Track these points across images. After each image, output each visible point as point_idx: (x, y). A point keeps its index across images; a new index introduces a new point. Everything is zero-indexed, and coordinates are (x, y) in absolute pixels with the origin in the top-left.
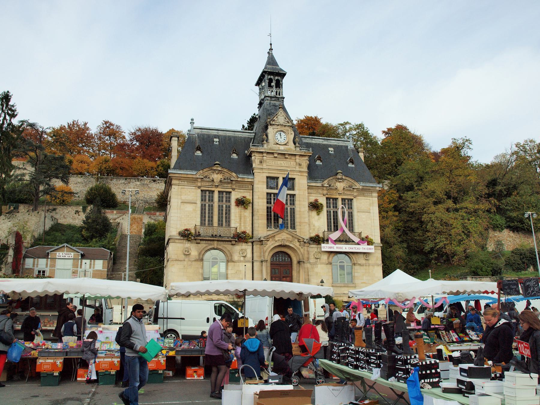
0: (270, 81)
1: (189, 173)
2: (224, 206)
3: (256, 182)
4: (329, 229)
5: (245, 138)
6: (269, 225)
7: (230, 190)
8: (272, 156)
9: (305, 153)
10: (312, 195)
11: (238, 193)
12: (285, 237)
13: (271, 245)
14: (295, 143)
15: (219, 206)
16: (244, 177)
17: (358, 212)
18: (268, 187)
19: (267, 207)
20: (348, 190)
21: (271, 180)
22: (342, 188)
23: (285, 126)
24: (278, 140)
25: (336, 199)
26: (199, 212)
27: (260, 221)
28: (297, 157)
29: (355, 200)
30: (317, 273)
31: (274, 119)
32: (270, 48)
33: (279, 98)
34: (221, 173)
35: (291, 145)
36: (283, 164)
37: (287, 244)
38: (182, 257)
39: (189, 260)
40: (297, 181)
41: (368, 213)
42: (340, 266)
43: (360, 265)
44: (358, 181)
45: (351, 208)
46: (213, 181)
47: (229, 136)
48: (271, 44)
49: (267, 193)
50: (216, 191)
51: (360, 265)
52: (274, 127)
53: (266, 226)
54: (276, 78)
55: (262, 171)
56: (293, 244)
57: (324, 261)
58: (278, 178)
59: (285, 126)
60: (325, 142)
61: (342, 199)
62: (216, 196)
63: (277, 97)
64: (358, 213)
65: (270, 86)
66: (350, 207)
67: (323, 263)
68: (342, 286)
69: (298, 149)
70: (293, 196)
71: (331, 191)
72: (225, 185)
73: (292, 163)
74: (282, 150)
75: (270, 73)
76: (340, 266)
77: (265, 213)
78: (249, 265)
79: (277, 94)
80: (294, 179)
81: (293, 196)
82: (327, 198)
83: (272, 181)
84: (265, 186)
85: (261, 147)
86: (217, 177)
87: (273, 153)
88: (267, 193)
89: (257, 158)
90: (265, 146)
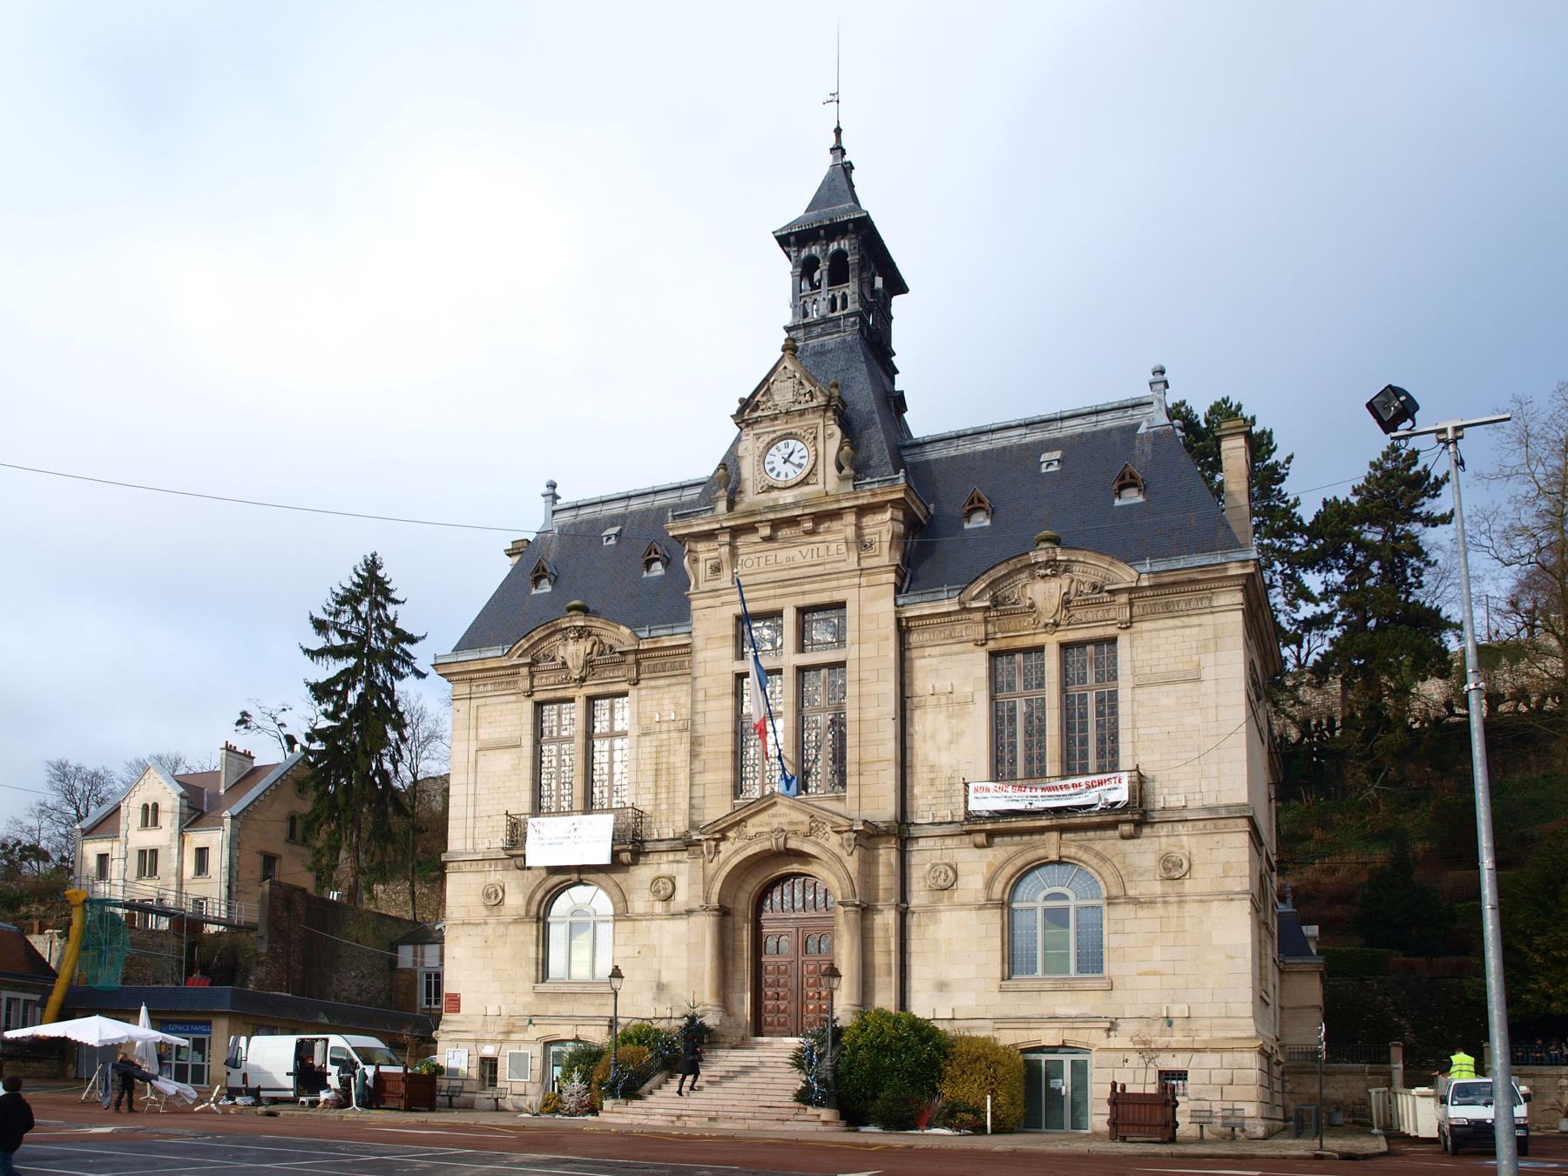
1: (489, 654)
3: (698, 641)
8: (755, 538)
9: (874, 495)
10: (928, 651)
11: (649, 692)
12: (783, 820)
14: (840, 468)
16: (661, 632)
17: (1139, 686)
20: (1087, 604)
22: (1056, 601)
23: (802, 413)
24: (773, 475)
31: (758, 398)
32: (832, 142)
33: (839, 318)
34: (590, 634)
36: (799, 559)
37: (793, 844)
40: (851, 609)
41: (1188, 686)
44: (1130, 559)
48: (838, 131)
53: (729, 790)
54: (834, 246)
55: (718, 601)
56: (817, 844)
59: (802, 413)
61: (1065, 647)
63: (831, 320)
64: (1138, 691)
68: (1047, 986)
71: (1013, 623)
72: (607, 674)
73: (833, 547)
74: (786, 507)
76: (1047, 911)
79: (833, 309)
80: (841, 605)
82: (994, 655)
84: (729, 651)
85: (709, 514)
86: (573, 652)
89: (702, 557)
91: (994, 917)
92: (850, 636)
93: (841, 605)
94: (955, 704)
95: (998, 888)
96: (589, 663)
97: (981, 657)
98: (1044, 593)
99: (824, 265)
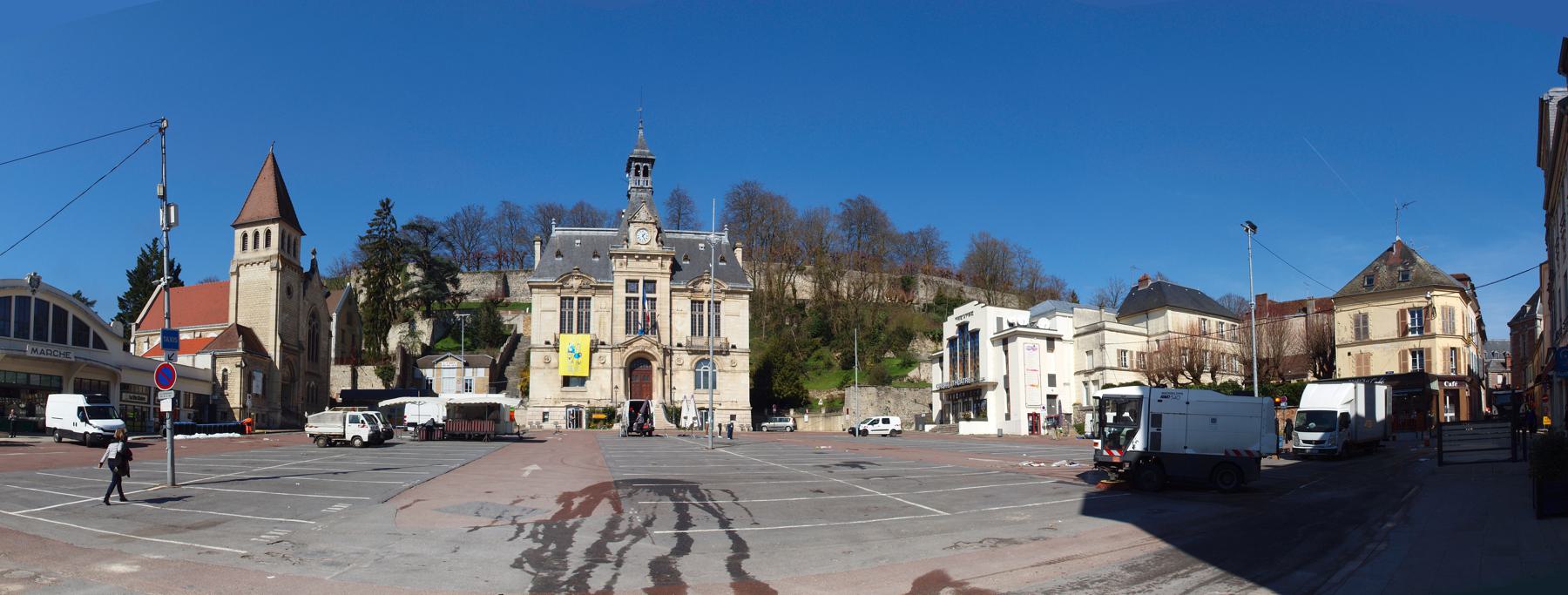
0: (638, 168)
2: (584, 312)
3: (615, 285)
4: (693, 333)
5: (608, 237)
6: (628, 331)
7: (590, 296)
13: (630, 351)
15: (578, 312)
18: (627, 292)
19: (627, 312)
21: (631, 284)
25: (702, 302)
26: (559, 320)
27: (619, 327)
28: (660, 258)
29: (723, 302)
30: (678, 380)
35: (654, 243)
36: (645, 266)
38: (543, 365)
39: (549, 368)
40: (657, 284)
42: (704, 372)
43: (725, 371)
44: (726, 281)
45: (719, 311)
46: (572, 287)
47: (592, 236)
49: (628, 299)
50: (576, 297)
51: (725, 371)
52: (637, 224)
57: (686, 368)
58: (638, 281)
60: (696, 237)
62: (575, 302)
65: (637, 174)
66: (718, 310)
67: (685, 370)
69: (660, 249)
70: (655, 299)
75: (637, 160)
76: (704, 372)
77: (624, 319)
78: (609, 372)
80: (655, 282)
81: (655, 299)
82: (693, 302)
83: (632, 284)
84: (625, 290)
87: (634, 255)
88: (628, 299)
90: (625, 246)
91: (692, 373)
92: (657, 291)
93: (655, 282)
94: (682, 312)
95: (693, 365)
96: (580, 287)
97: (689, 301)
98: (705, 286)
99: (642, 169)
